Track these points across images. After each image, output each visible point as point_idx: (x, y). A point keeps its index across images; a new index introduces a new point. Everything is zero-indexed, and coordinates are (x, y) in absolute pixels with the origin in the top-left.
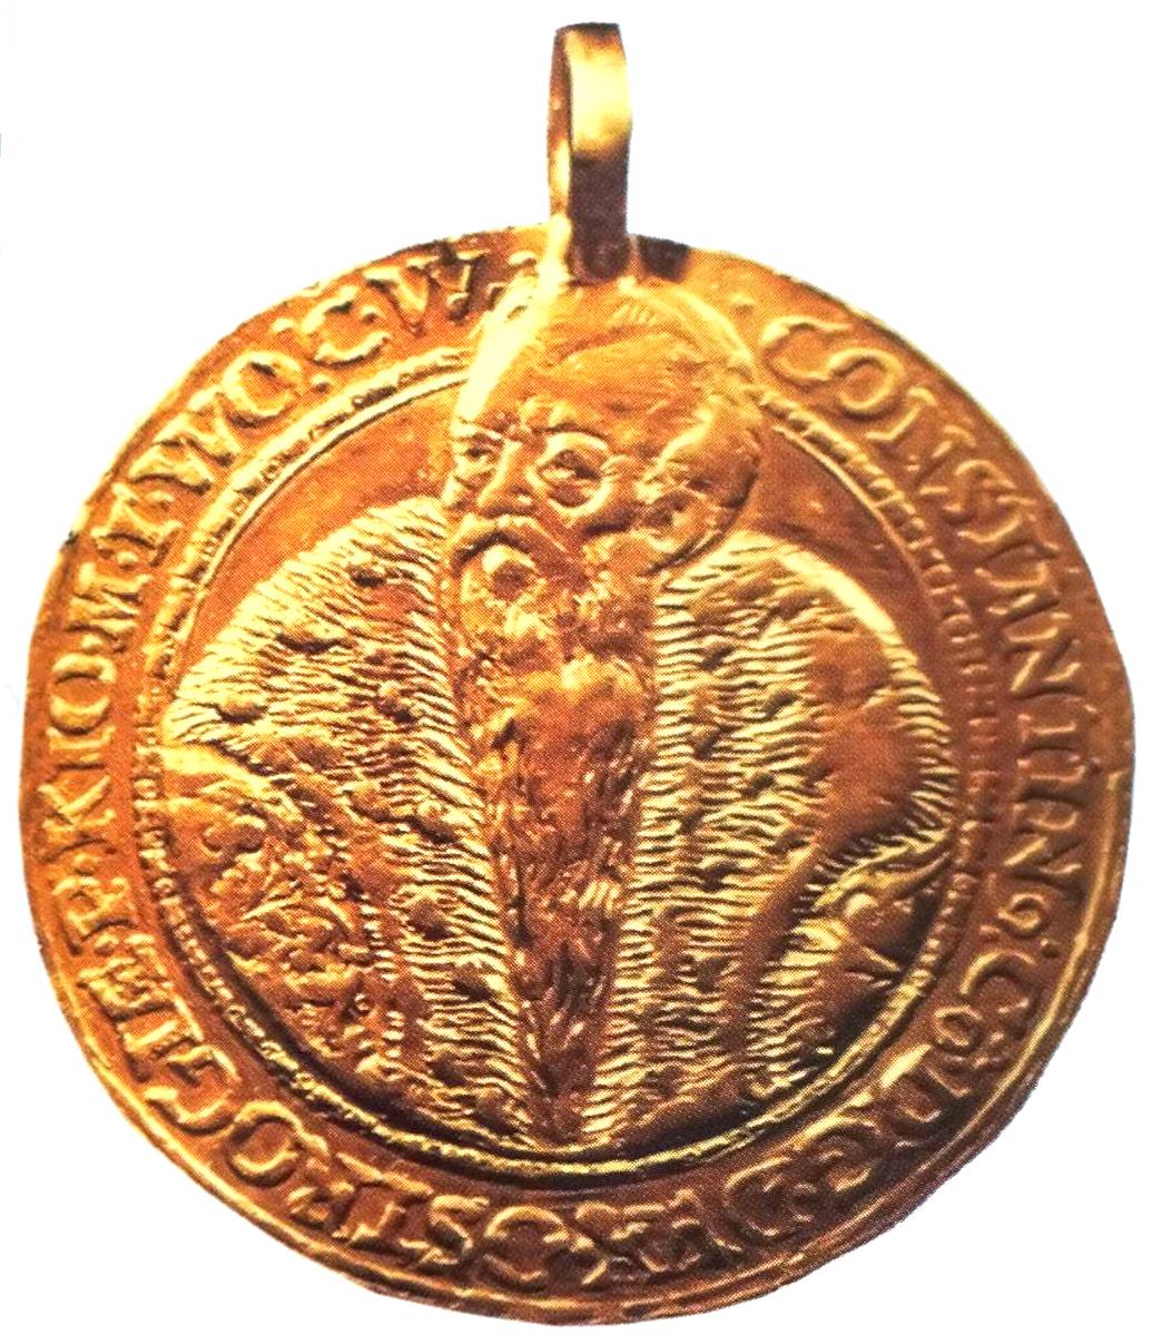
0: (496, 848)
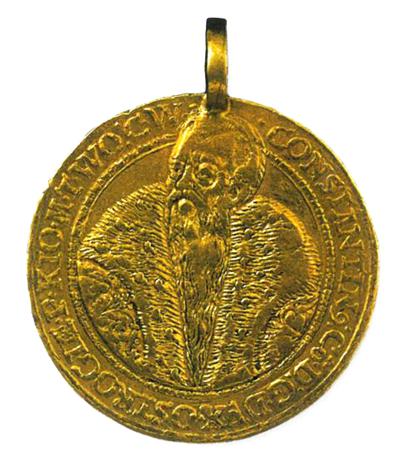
0: (179, 294)
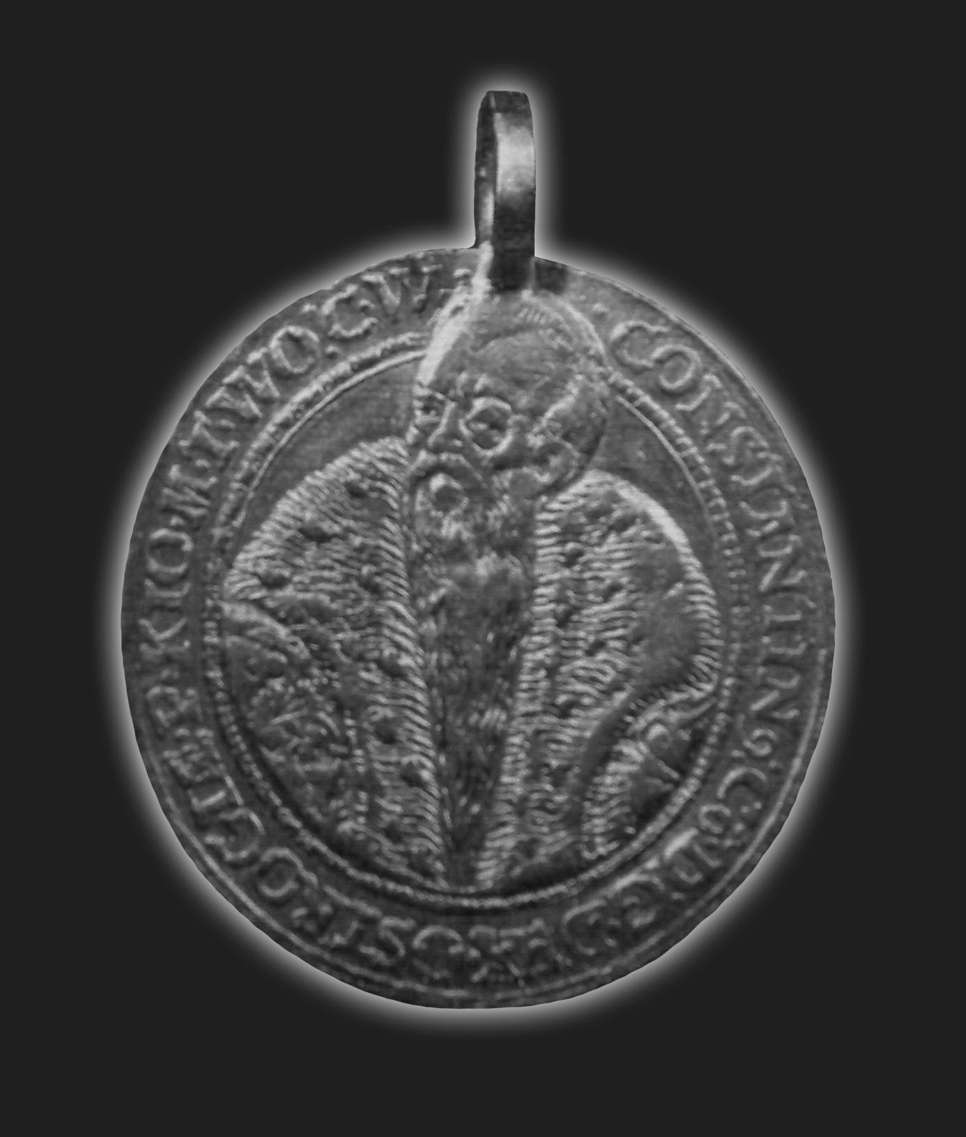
0: (430, 683)
